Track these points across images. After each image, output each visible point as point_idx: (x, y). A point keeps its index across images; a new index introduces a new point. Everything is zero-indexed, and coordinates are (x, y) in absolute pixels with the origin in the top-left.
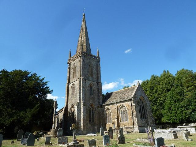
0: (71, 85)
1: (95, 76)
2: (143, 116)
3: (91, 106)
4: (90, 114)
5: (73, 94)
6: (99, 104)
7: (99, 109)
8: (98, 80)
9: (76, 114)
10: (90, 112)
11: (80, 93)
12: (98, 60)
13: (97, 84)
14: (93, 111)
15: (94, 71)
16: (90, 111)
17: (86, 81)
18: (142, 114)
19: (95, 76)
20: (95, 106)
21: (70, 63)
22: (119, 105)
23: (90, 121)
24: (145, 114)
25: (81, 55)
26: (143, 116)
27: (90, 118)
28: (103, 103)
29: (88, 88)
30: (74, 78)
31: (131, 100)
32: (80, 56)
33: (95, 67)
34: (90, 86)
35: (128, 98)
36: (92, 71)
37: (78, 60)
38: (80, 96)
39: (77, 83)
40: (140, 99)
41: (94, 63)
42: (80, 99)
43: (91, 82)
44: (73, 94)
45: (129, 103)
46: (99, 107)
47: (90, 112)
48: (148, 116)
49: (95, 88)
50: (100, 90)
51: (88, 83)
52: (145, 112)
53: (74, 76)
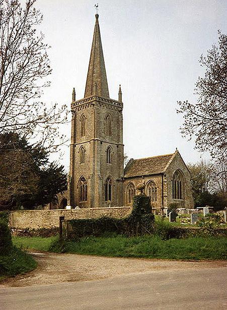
0: (78, 147)
2: (177, 196)
3: (108, 179)
4: (106, 190)
5: (82, 161)
8: (119, 141)
9: (89, 190)
12: (119, 106)
13: (118, 147)
14: (110, 186)
16: (106, 185)
17: (101, 143)
18: (177, 193)
20: (116, 178)
21: (74, 110)
22: (147, 180)
26: (177, 196)
28: (124, 174)
30: (82, 135)
31: (162, 174)
32: (94, 105)
39: (88, 146)
44: (82, 161)
45: (160, 178)
50: (121, 157)
51: (105, 146)
52: (182, 190)
53: (82, 134)
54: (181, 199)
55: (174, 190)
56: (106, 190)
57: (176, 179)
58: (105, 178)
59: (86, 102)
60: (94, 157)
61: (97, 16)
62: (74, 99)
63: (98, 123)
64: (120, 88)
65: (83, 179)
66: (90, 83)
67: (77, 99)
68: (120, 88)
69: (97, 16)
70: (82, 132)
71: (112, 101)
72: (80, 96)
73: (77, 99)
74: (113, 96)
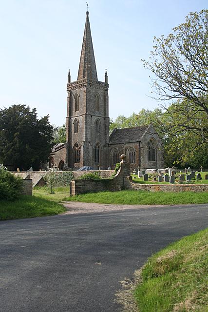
1: (102, 109)
3: (97, 145)
4: (96, 154)
5: (76, 131)
6: (106, 143)
7: (105, 148)
8: (105, 114)
10: (96, 152)
11: (86, 131)
12: (105, 86)
14: (98, 150)
15: (101, 103)
16: (96, 150)
19: (102, 109)
20: (103, 145)
21: (70, 89)
23: (95, 161)
24: (154, 156)
25: (86, 84)
27: (96, 158)
29: (94, 125)
32: (85, 86)
33: (102, 98)
34: (97, 122)
35: (137, 140)
36: (98, 103)
37: (81, 89)
38: (86, 134)
39: (81, 119)
40: (151, 140)
41: (101, 92)
42: (86, 138)
43: (97, 118)
44: (76, 131)
45: (138, 144)
46: (105, 146)
47: (96, 152)
48: (158, 159)
49: (101, 124)
51: (94, 119)
52: (155, 154)
54: (154, 160)
55: (149, 153)
56: (96, 154)
57: (151, 145)
58: (94, 144)
59: (78, 85)
60: (86, 128)
61: (87, 13)
62: (69, 80)
63: (88, 101)
64: (106, 72)
65: (76, 145)
66: (82, 69)
67: (72, 81)
68: (106, 72)
69: (87, 13)
70: (76, 108)
71: (100, 82)
72: (74, 79)
73: (72, 81)
74: (101, 78)
